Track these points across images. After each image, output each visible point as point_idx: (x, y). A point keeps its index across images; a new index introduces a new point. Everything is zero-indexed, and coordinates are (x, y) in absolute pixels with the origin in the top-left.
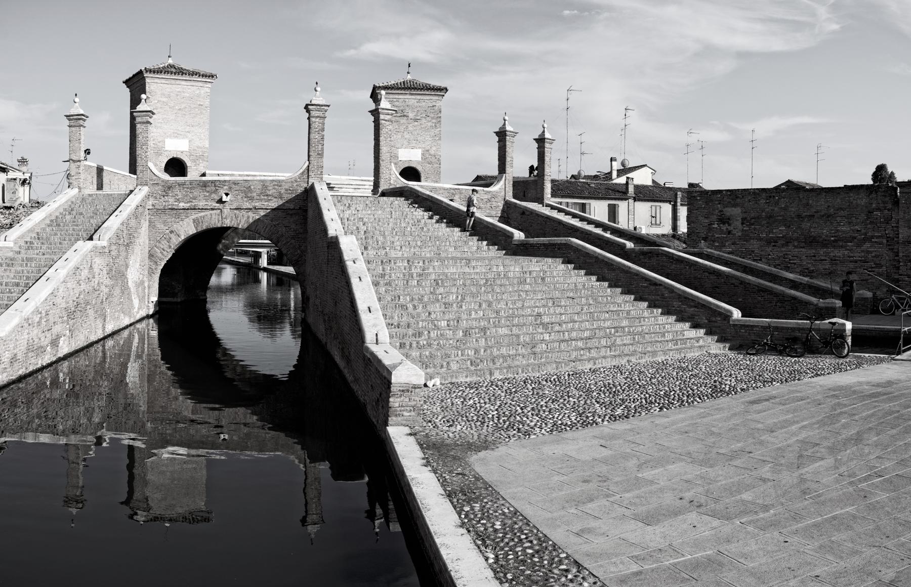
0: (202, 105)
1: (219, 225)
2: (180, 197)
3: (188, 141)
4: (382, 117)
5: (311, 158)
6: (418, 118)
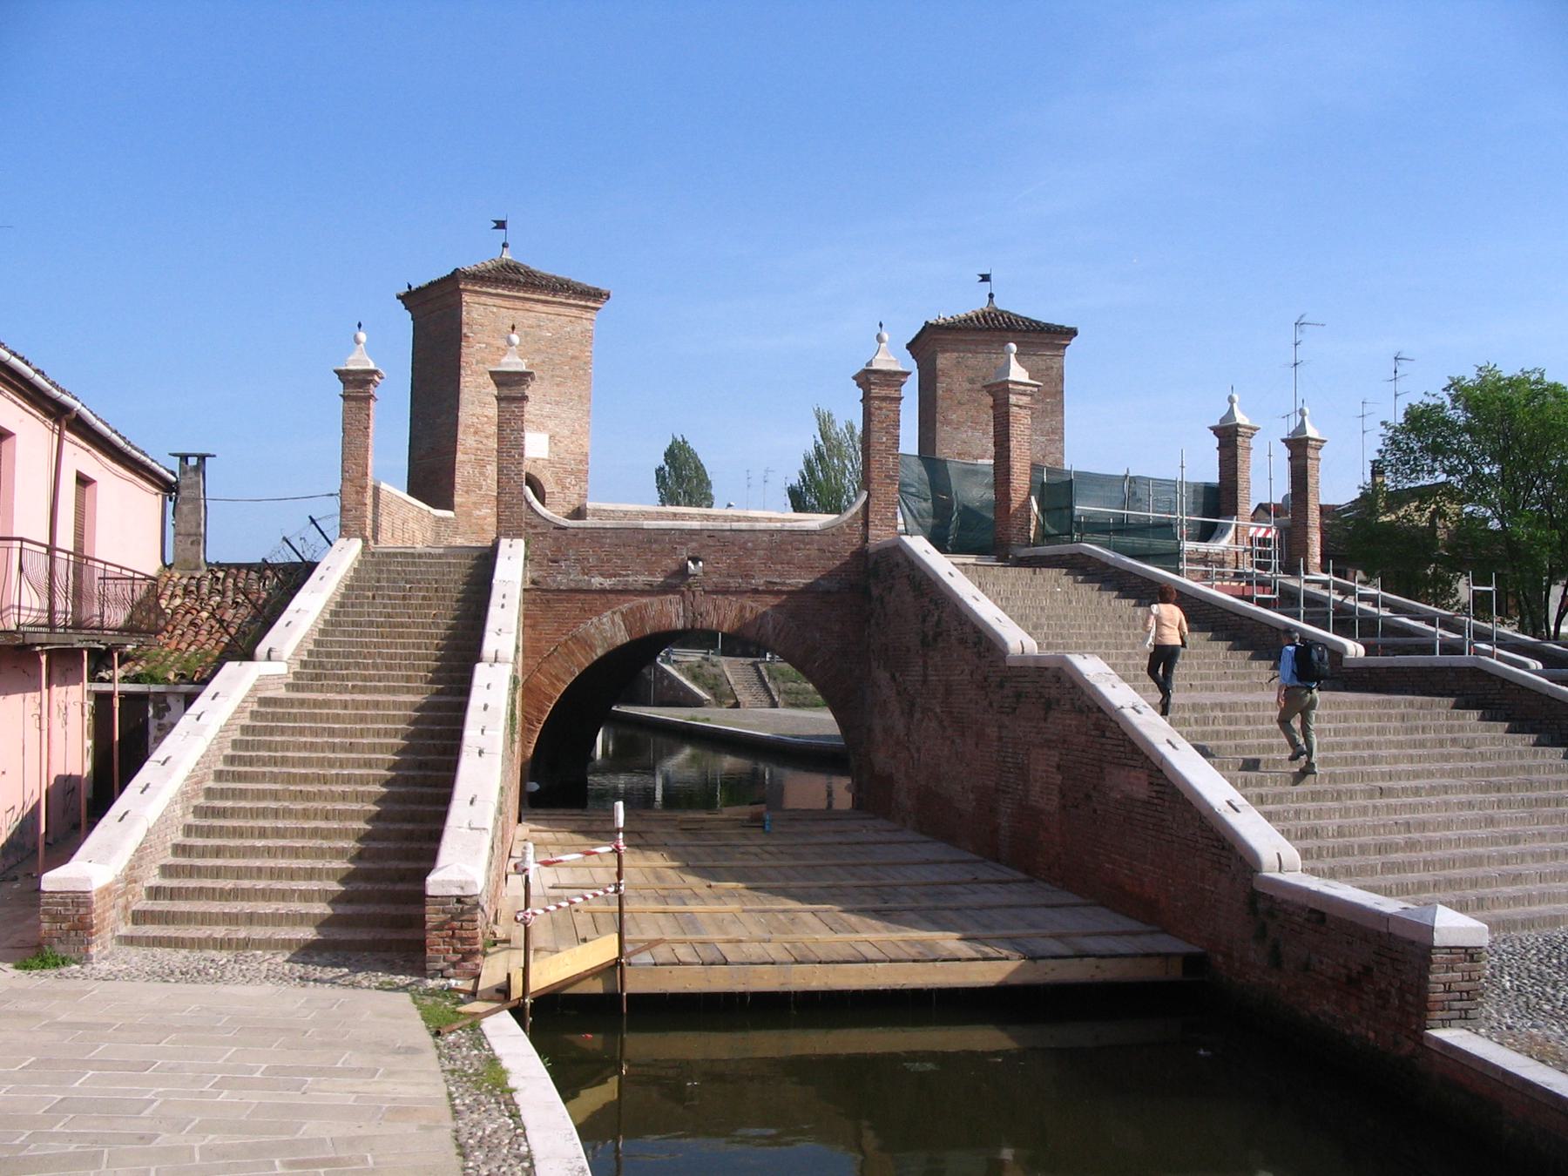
3: (547, 436)
4: (1013, 399)
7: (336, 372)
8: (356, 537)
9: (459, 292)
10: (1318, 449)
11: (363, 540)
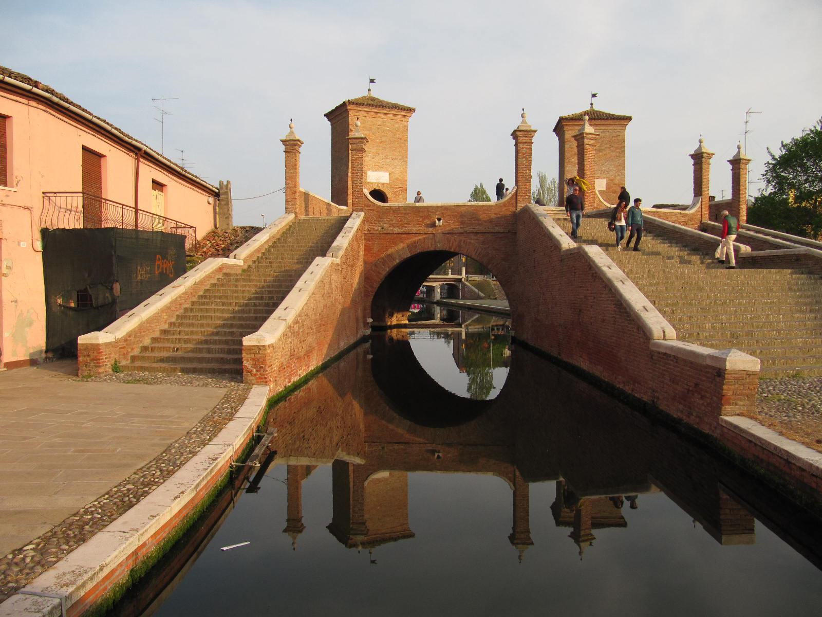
0: (401, 139)
1: (432, 249)
2: (394, 222)
3: (387, 174)
4: (586, 141)
5: (520, 184)
6: (602, 148)
7: (282, 141)
8: (292, 213)
9: (347, 111)
10: (748, 163)
11: (295, 214)
